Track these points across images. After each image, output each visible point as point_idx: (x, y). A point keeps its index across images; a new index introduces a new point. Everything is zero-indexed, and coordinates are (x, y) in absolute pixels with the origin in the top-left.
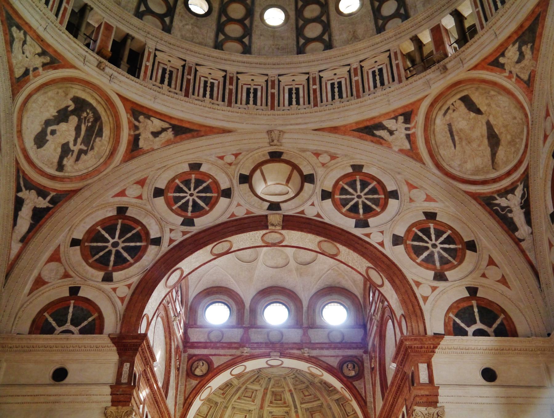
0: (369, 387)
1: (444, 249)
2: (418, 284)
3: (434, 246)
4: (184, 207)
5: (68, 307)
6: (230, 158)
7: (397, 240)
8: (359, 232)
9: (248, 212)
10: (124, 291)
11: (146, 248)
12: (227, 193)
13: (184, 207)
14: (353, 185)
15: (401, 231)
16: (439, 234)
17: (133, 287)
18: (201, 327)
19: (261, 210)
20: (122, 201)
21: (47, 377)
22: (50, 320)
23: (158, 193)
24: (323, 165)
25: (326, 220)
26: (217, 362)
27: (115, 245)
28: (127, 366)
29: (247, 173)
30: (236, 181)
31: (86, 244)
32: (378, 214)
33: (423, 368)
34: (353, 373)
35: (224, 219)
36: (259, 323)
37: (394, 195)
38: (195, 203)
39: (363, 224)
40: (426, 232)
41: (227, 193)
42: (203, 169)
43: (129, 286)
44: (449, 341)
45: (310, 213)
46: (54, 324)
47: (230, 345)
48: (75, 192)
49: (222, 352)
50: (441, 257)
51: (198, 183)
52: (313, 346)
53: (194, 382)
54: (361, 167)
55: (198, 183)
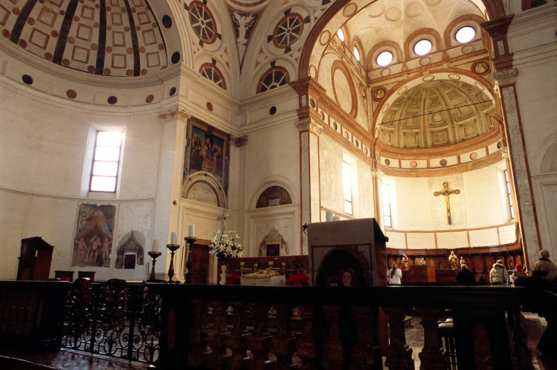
5: (272, 74)
18: (376, 69)
22: (264, 85)
26: (388, 88)
27: (288, 31)
28: (304, 97)
31: (276, 37)
46: (266, 86)
47: (395, 76)
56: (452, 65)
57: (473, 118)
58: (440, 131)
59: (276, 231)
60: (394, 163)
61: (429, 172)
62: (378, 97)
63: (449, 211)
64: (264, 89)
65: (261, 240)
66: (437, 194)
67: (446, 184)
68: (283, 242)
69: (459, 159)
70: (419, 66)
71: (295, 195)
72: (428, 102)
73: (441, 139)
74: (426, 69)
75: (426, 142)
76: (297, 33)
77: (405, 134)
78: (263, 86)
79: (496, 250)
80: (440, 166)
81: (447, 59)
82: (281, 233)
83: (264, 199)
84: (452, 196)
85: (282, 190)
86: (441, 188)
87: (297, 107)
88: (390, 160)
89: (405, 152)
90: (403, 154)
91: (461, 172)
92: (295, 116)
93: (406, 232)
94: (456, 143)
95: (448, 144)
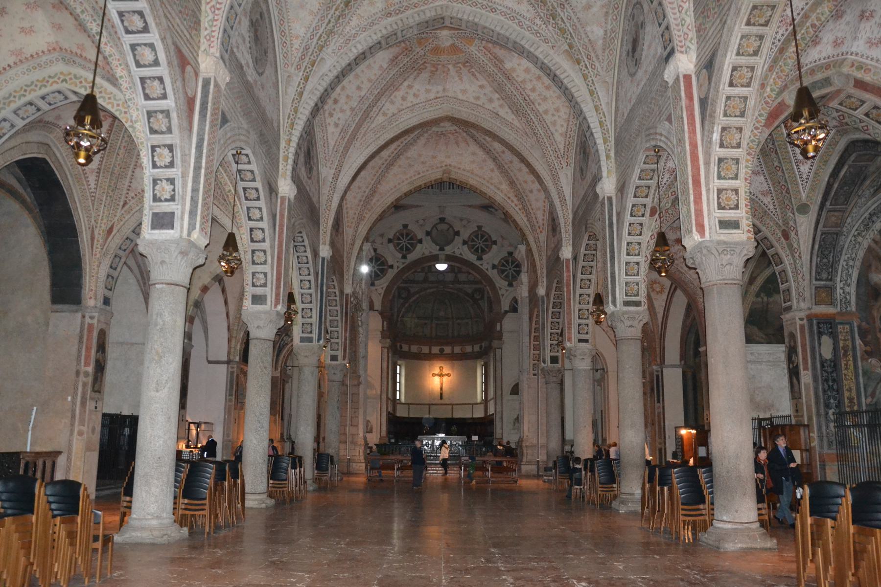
0: (486, 305)
1: (514, 271)
2: (500, 289)
3: (510, 269)
6: (421, 222)
7: (494, 267)
8: (478, 263)
9: (430, 252)
11: (387, 270)
12: (420, 241)
13: (401, 248)
14: (477, 237)
15: (496, 263)
16: (513, 263)
17: (384, 288)
23: (390, 241)
24: (464, 226)
25: (465, 257)
26: (412, 290)
29: (429, 230)
32: (487, 253)
33: (498, 324)
34: (479, 297)
36: (434, 270)
37: (495, 243)
39: (480, 258)
40: (507, 262)
42: (409, 228)
44: (510, 315)
45: (457, 254)
49: (415, 285)
50: (512, 275)
51: (407, 235)
52: (459, 283)
53: (402, 301)
54: (482, 227)
55: (407, 235)
60: (405, 348)
62: (403, 296)
63: (441, 389)
66: (434, 375)
80: (439, 353)
84: (445, 379)
87: (381, 329)
93: (409, 404)
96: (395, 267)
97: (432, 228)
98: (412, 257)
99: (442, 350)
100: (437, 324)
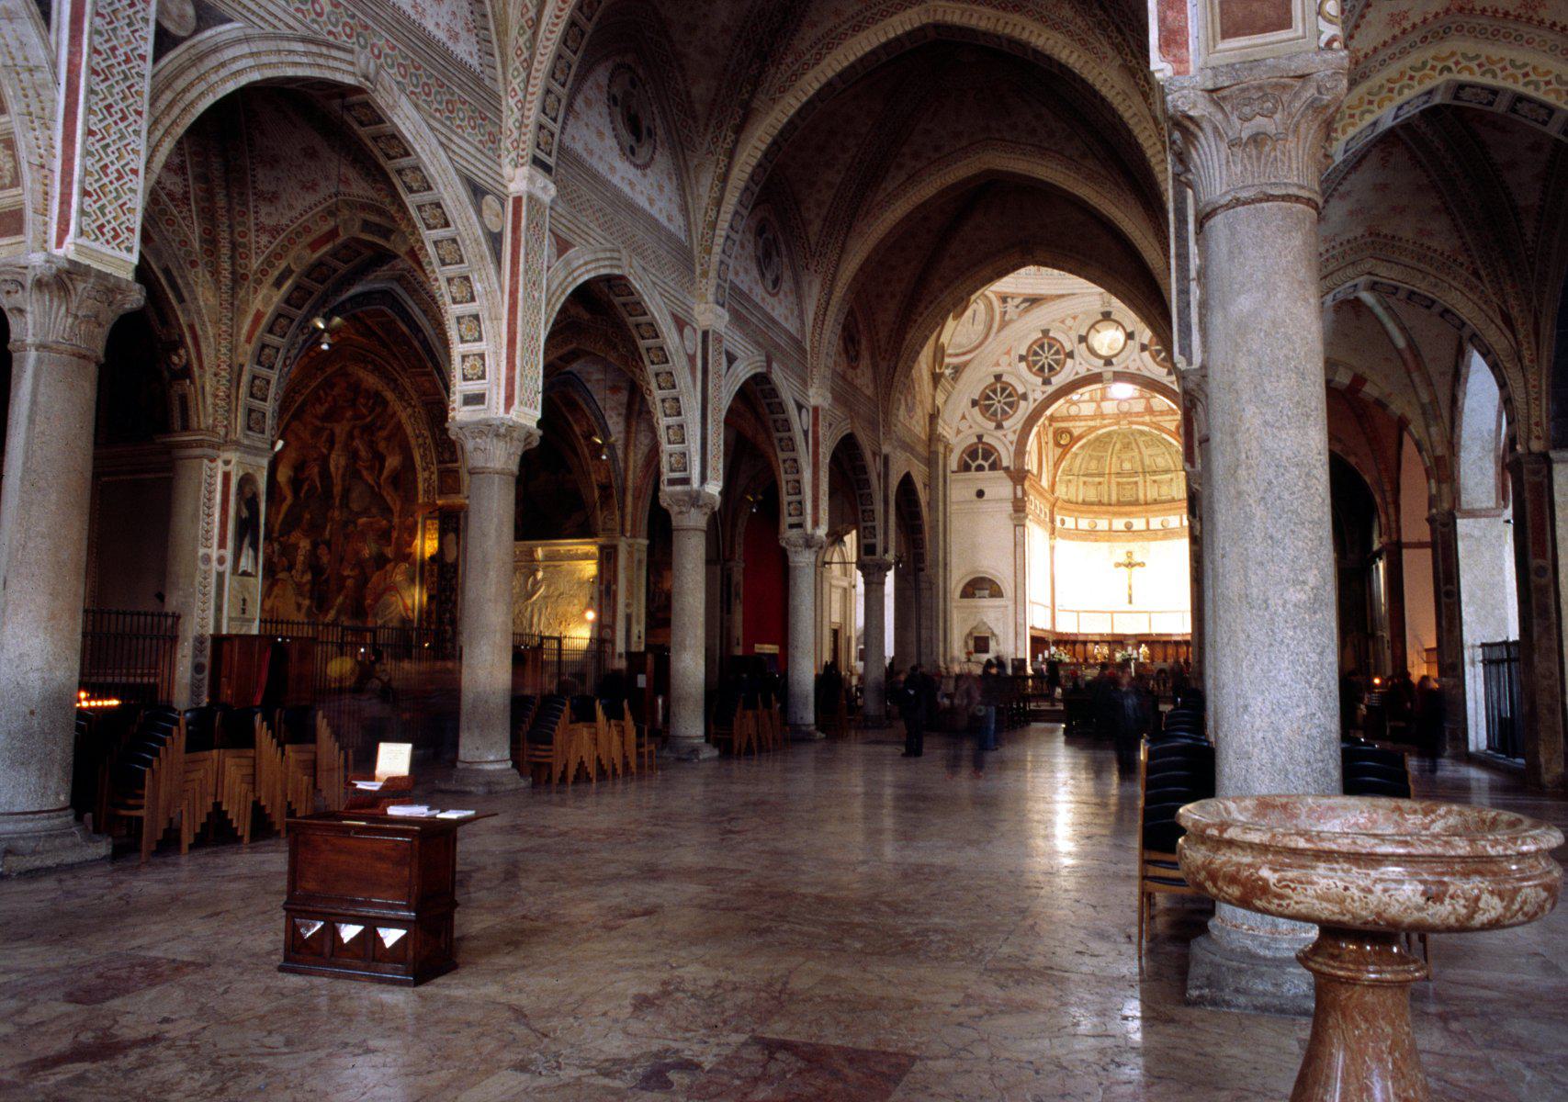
4: (1042, 369)
10: (1014, 438)
12: (1070, 355)
19: (1098, 365)
20: (998, 370)
21: (975, 498)
23: (1022, 358)
26: (1076, 432)
28: (1019, 488)
29: (1083, 333)
30: (1076, 339)
35: (1072, 378)
38: (1050, 366)
41: (1070, 355)
43: (1015, 432)
45: (1133, 369)
47: (1086, 418)
48: (966, 364)
49: (1078, 424)
53: (1060, 450)
56: (1154, 419)
57: (1169, 476)
58: (1129, 483)
59: (985, 624)
60: (1070, 523)
61: (1111, 535)
64: (966, 468)
65: (967, 631)
66: (1118, 565)
67: (1130, 554)
68: (993, 634)
69: (1148, 523)
70: (1116, 411)
71: (1008, 588)
72: (1118, 446)
73: (1128, 495)
74: (1125, 418)
75: (1110, 495)
76: (1011, 407)
77: (1085, 483)
78: (966, 462)
79: (1179, 638)
81: (1150, 410)
82: (992, 625)
83: (970, 590)
84: (1136, 569)
85: (991, 582)
86: (1123, 559)
87: (1012, 496)
88: (1066, 519)
89: (1084, 508)
90: (1081, 512)
91: (1148, 540)
92: (1009, 508)
94: (1146, 504)
95: (1136, 503)
96: (1031, 399)
97: (1088, 333)
98: (1058, 381)
99: (1129, 527)
100: (1118, 484)
